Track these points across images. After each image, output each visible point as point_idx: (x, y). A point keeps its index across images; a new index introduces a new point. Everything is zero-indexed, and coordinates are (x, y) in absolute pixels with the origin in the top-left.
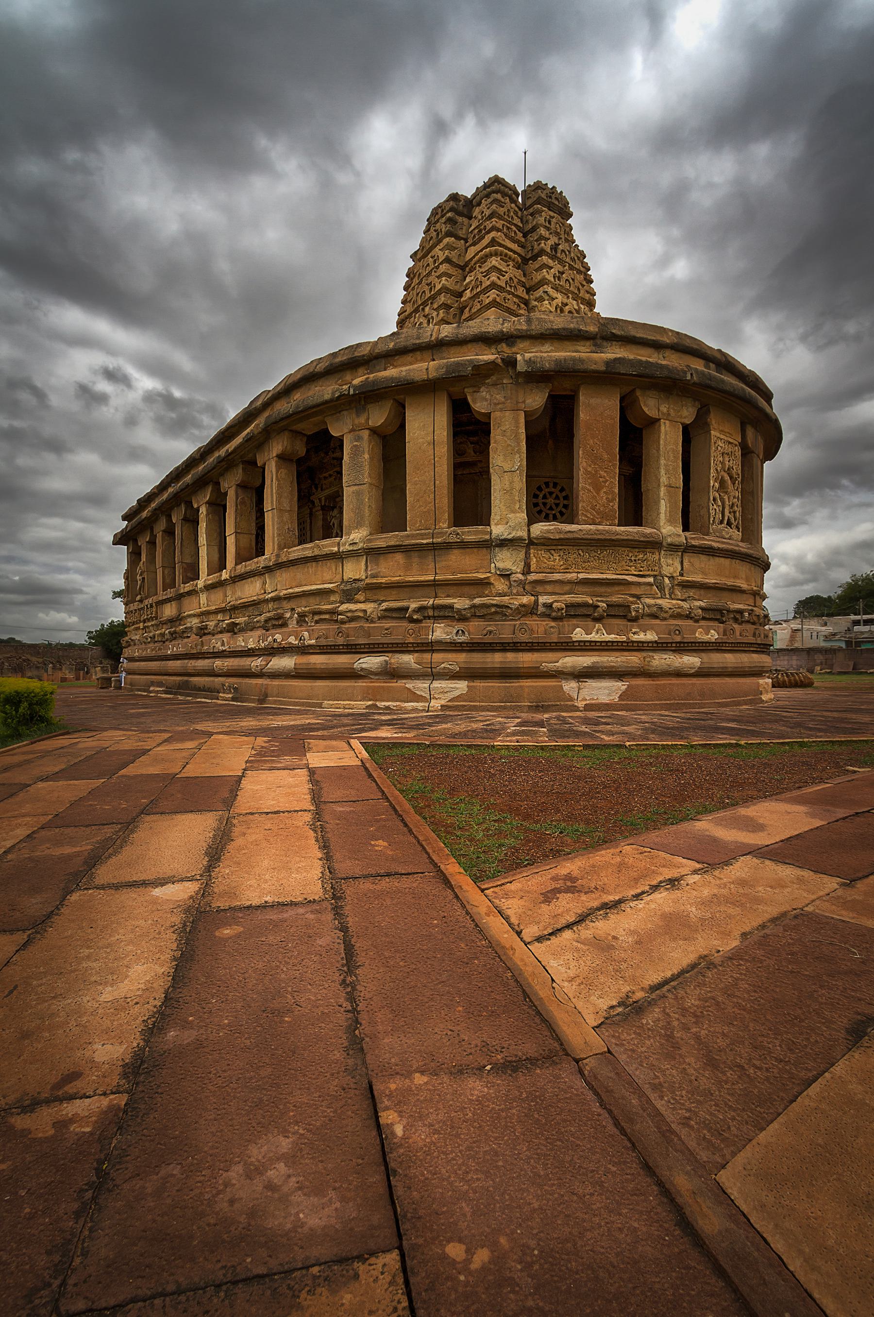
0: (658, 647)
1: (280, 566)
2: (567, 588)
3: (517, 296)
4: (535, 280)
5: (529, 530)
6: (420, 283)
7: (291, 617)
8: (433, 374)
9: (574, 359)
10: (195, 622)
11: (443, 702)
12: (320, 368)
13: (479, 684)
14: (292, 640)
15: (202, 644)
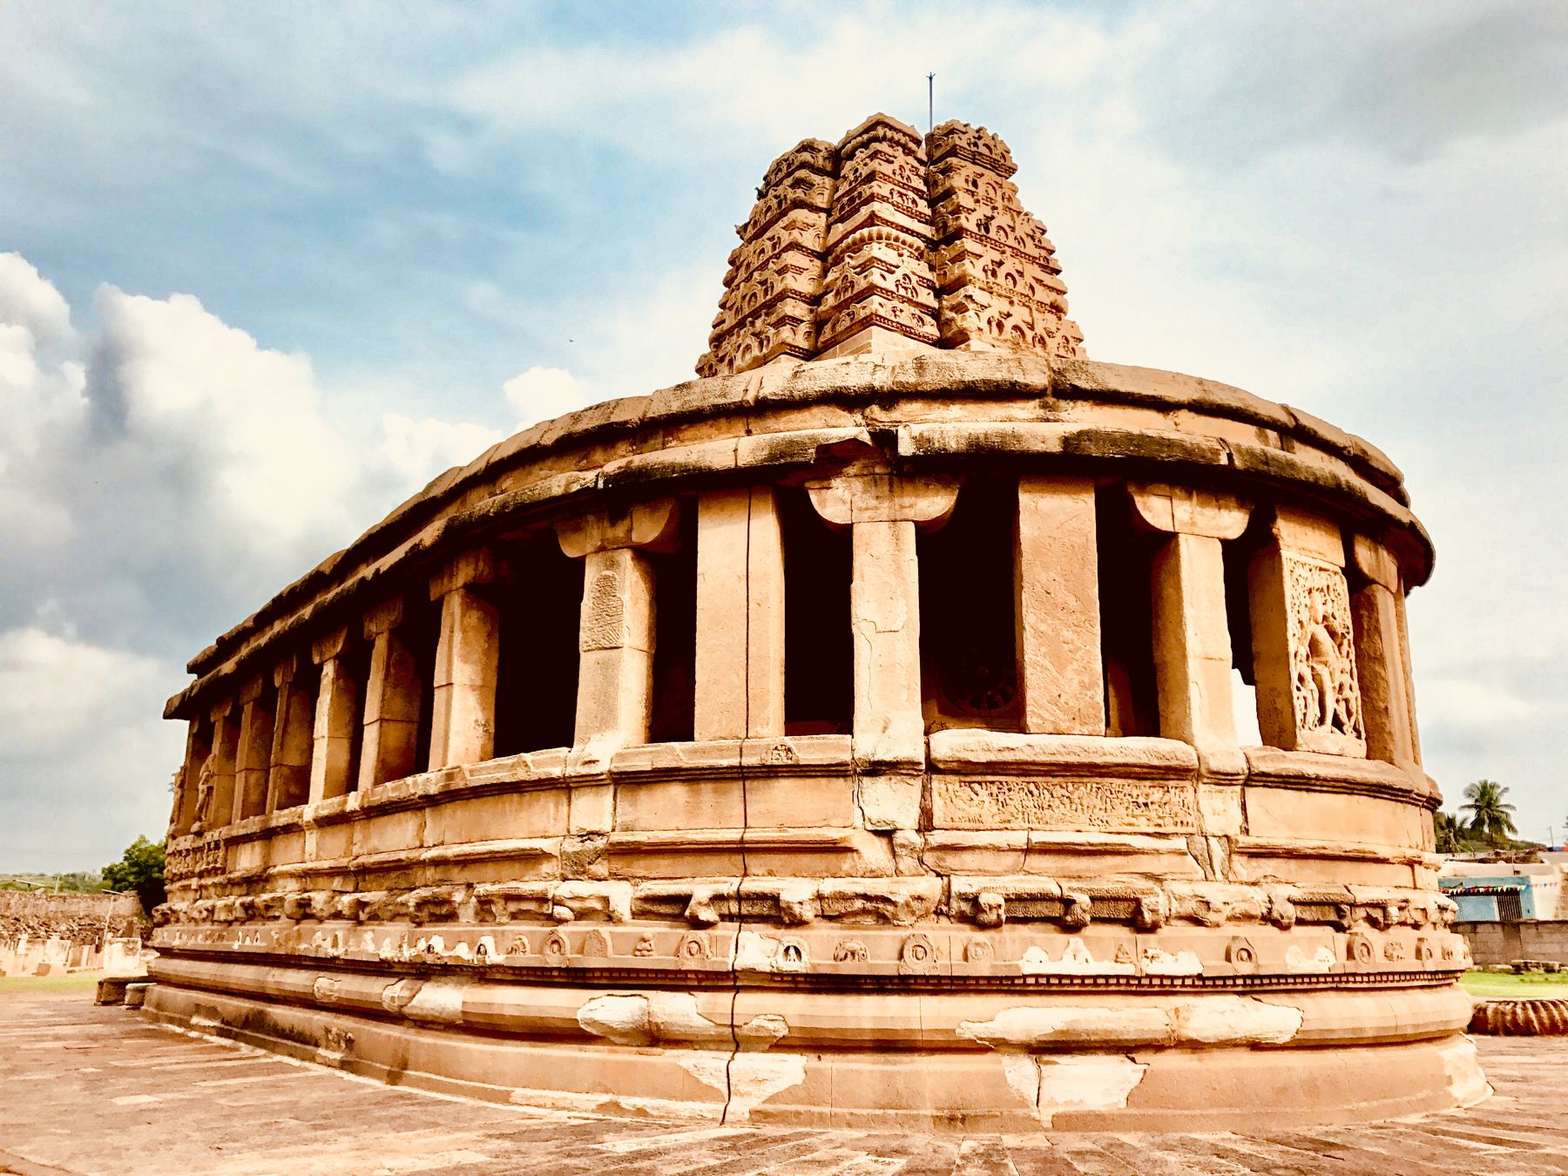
0: (1204, 985)
2: (1010, 859)
3: (918, 305)
4: (951, 277)
5: (928, 744)
6: (748, 279)
7: (464, 903)
8: (745, 459)
9: (1003, 436)
10: (289, 891)
11: (756, 1103)
12: (548, 440)
13: (832, 1063)
14: (464, 953)
15: (299, 937)
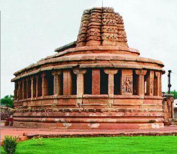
0: (107, 117)
1: (45, 99)
13: (74, 124)
